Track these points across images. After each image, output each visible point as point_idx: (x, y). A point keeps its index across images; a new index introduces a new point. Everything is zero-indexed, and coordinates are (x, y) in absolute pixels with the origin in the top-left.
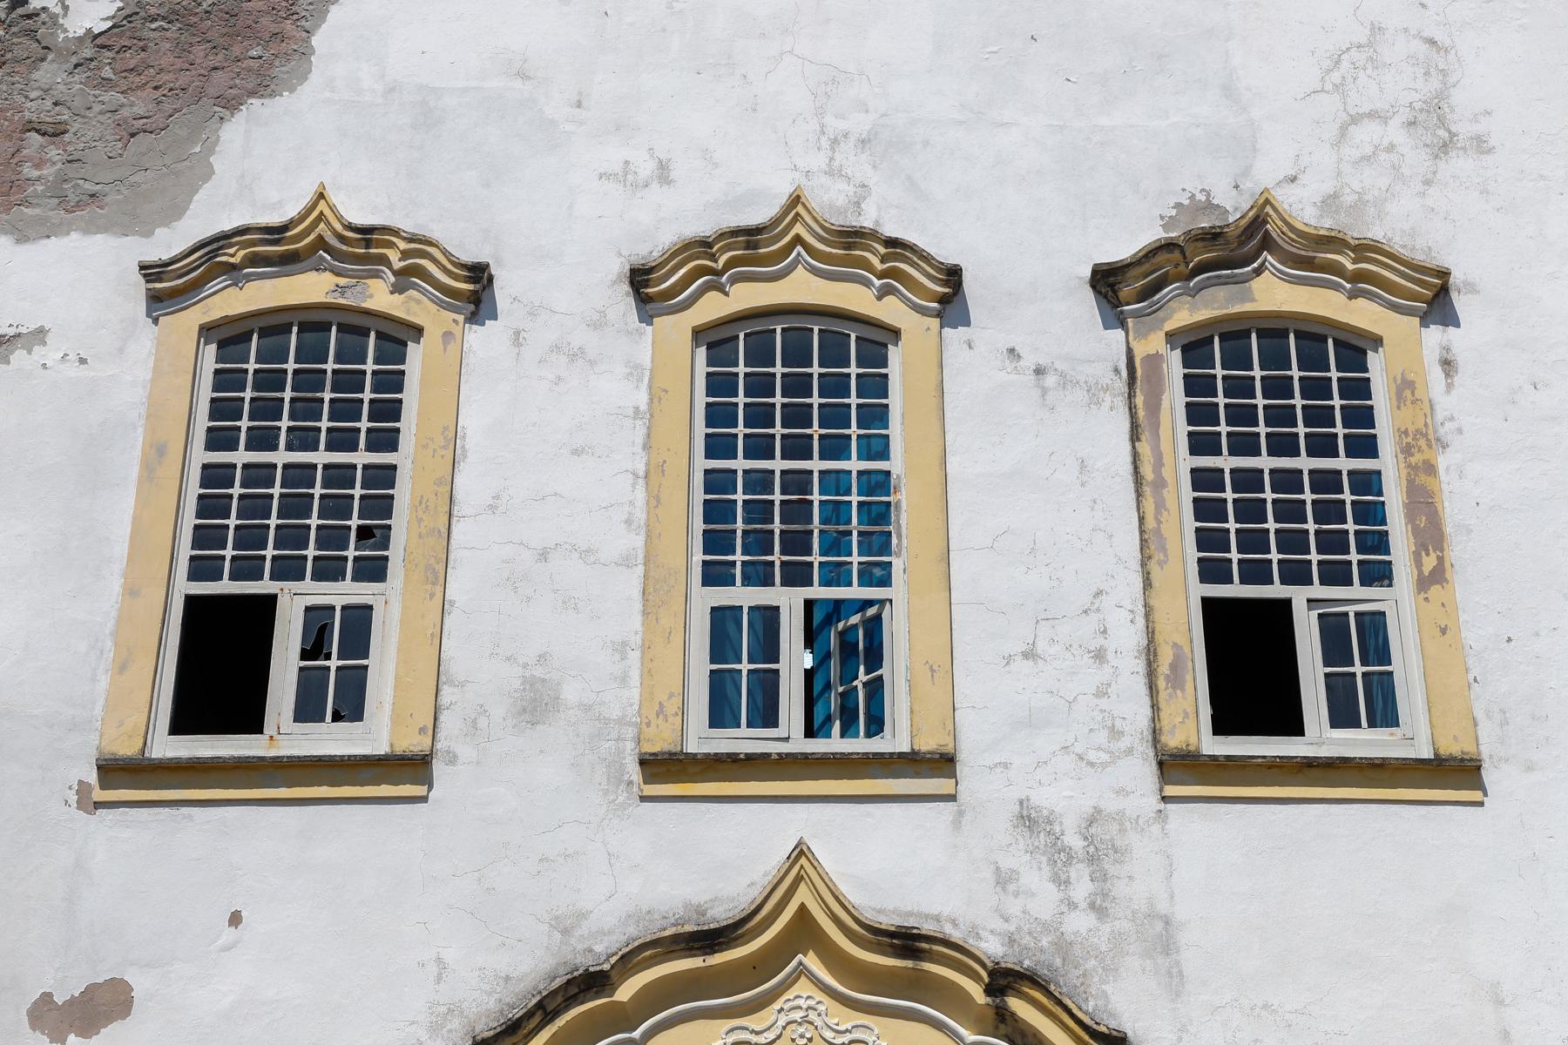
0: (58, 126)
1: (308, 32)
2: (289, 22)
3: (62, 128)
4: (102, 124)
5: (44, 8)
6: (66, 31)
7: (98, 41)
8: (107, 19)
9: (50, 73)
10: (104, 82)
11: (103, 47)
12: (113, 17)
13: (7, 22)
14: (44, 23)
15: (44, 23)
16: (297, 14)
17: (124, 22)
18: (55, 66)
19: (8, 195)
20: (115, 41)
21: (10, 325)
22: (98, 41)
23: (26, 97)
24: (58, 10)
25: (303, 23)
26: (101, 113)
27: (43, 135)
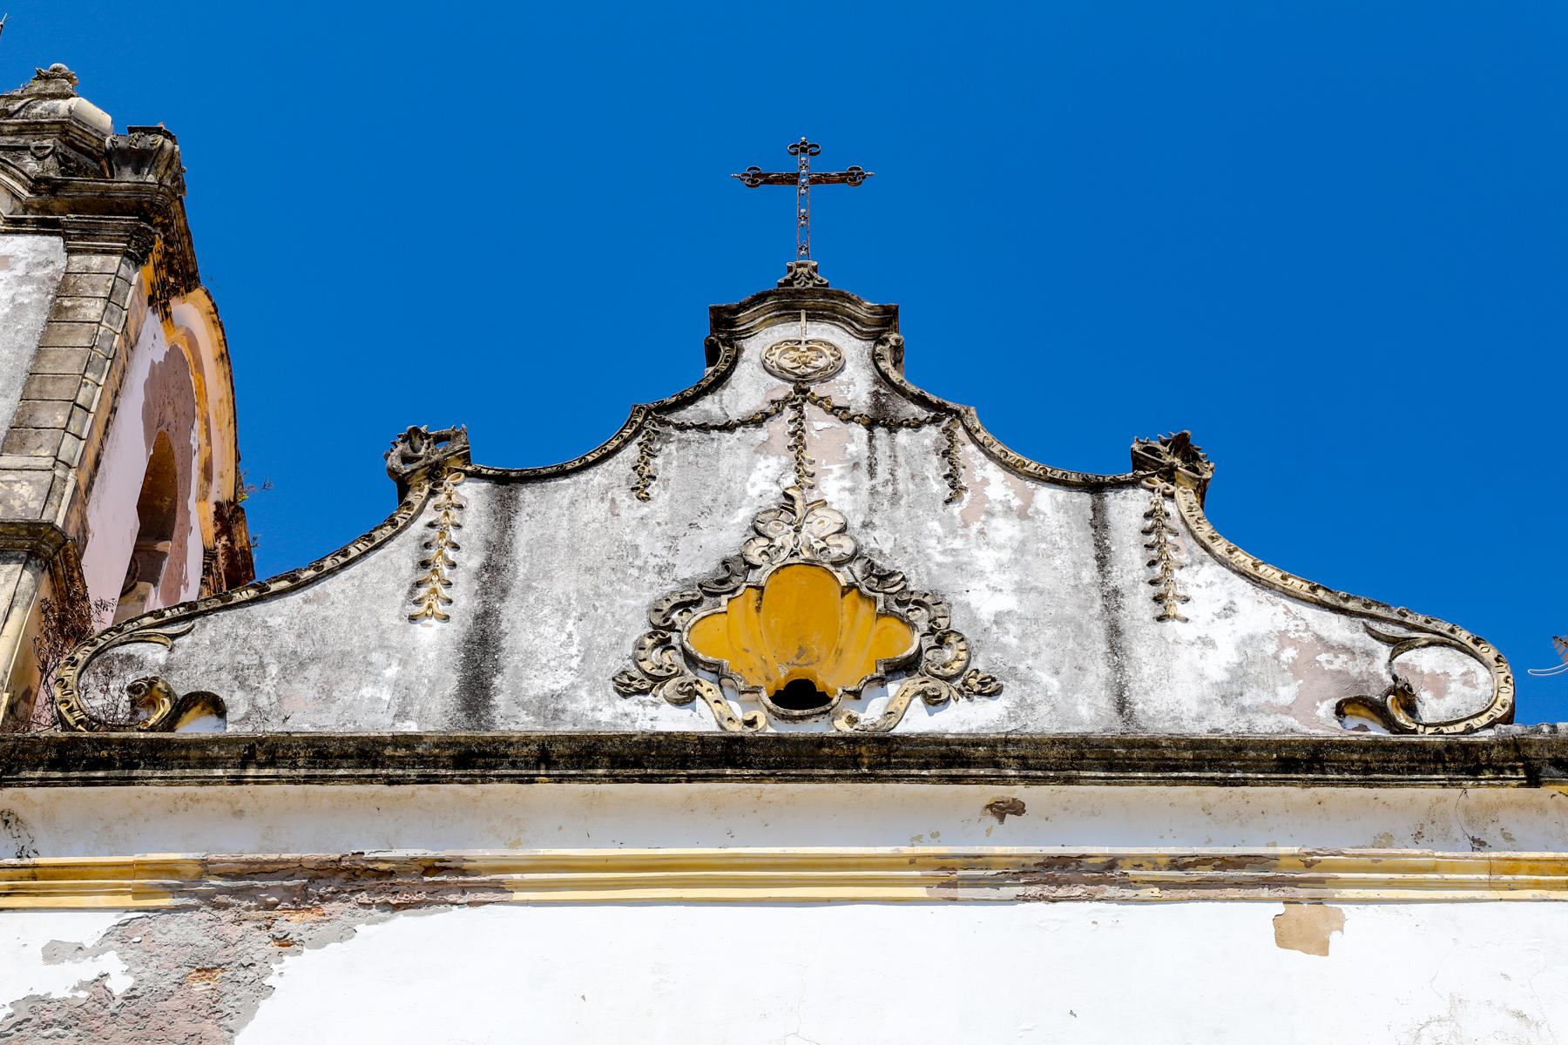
1: (232, 1031)
2: (209, 1021)
16: (221, 1011)
25: (227, 1021)
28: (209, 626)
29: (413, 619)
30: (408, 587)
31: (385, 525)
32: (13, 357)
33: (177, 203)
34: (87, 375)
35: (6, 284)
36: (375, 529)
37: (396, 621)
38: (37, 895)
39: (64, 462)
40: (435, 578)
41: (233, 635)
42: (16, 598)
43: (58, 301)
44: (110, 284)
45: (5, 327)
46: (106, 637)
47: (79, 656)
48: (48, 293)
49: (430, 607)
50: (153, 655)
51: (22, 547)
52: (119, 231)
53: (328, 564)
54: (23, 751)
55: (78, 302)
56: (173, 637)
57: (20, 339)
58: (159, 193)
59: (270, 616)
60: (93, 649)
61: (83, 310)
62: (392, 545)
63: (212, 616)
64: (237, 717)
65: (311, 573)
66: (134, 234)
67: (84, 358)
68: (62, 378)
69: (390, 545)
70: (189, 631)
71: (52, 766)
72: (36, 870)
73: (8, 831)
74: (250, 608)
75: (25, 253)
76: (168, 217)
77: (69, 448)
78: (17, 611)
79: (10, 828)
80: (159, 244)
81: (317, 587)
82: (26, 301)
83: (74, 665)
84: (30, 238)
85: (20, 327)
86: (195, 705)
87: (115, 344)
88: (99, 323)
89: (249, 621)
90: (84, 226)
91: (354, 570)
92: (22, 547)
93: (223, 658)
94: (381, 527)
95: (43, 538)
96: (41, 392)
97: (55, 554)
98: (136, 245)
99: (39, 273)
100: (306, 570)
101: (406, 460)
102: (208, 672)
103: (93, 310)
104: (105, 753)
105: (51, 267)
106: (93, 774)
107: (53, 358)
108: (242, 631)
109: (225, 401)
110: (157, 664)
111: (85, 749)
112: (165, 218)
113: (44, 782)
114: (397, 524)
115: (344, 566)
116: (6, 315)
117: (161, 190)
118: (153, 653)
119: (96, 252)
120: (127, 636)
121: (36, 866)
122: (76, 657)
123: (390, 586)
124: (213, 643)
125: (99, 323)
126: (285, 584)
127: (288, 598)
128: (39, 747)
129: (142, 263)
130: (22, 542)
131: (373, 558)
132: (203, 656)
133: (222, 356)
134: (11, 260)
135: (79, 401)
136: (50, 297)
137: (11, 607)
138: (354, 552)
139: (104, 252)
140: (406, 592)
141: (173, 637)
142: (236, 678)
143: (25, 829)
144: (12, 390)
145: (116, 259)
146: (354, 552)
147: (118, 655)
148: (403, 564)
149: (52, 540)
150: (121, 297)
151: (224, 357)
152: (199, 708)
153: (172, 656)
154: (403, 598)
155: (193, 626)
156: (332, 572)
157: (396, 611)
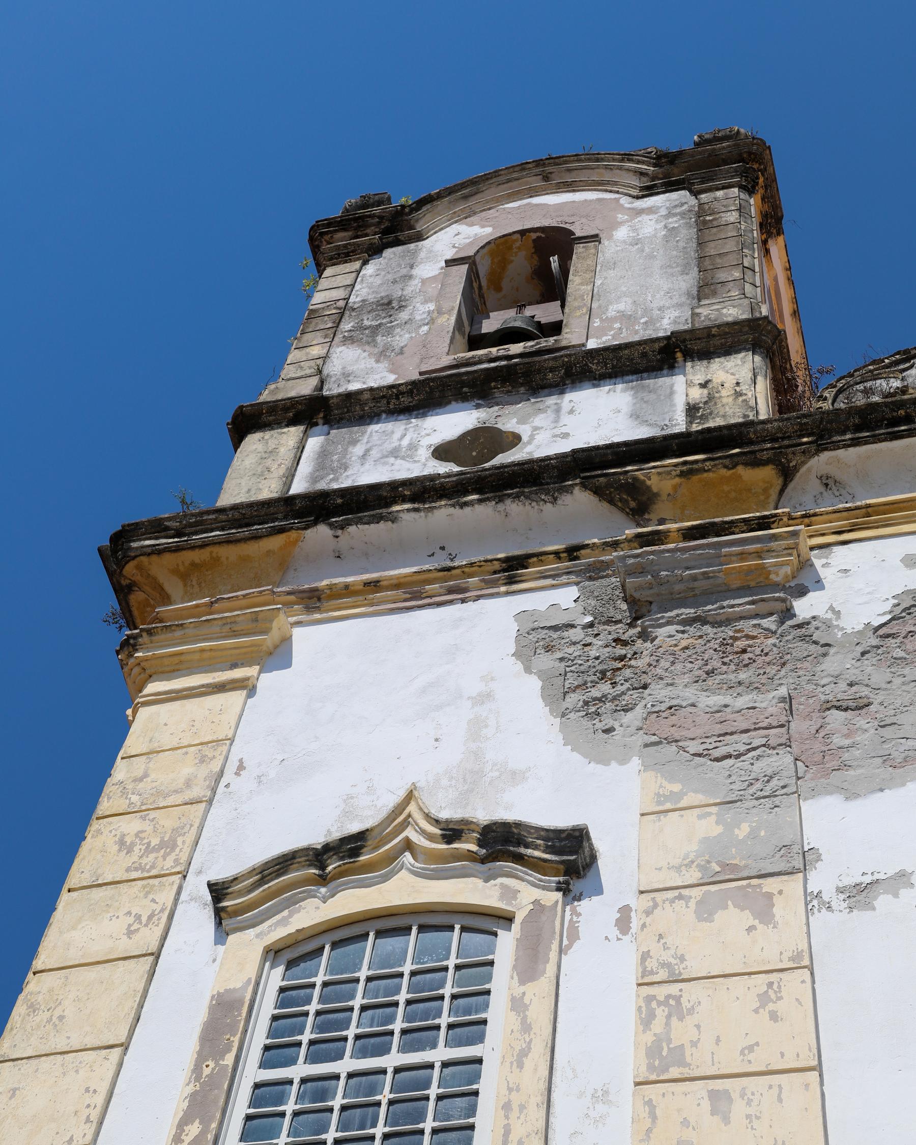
0: (860, 700)
3: (865, 701)
4: (908, 692)
5: (814, 617)
6: (843, 629)
7: (881, 632)
8: (884, 614)
9: (832, 664)
10: (899, 661)
11: (888, 636)
12: (890, 612)
13: (779, 631)
14: (817, 628)
15: (817, 628)
17: (904, 614)
18: (839, 656)
19: (823, 763)
20: (898, 629)
21: (864, 874)
22: (881, 632)
23: (816, 685)
24: (830, 615)
26: (904, 684)
27: (846, 709)
32: (681, 254)
33: (768, 152)
38: (877, 527)
42: (756, 371)
48: (691, 218)
51: (746, 341)
52: (731, 173)
54: (830, 422)
58: (753, 145)
60: (835, 390)
66: (744, 173)
71: (858, 428)
72: (870, 510)
73: (830, 492)
76: (763, 163)
78: (760, 379)
79: (830, 489)
80: (761, 180)
84: (662, 196)
88: (739, 222)
90: (703, 175)
92: (746, 341)
95: (762, 331)
96: (713, 264)
97: (773, 344)
98: (746, 180)
104: (902, 412)
106: (896, 429)
109: (800, 351)
111: (884, 411)
112: (760, 164)
113: (855, 443)
117: (755, 141)
119: (718, 189)
121: (868, 506)
122: (825, 395)
125: (739, 222)
128: (843, 417)
129: (753, 192)
130: (746, 337)
133: (795, 312)
135: (746, 264)
139: (724, 188)
143: (844, 489)
145: (736, 190)
149: (769, 332)
151: (795, 313)
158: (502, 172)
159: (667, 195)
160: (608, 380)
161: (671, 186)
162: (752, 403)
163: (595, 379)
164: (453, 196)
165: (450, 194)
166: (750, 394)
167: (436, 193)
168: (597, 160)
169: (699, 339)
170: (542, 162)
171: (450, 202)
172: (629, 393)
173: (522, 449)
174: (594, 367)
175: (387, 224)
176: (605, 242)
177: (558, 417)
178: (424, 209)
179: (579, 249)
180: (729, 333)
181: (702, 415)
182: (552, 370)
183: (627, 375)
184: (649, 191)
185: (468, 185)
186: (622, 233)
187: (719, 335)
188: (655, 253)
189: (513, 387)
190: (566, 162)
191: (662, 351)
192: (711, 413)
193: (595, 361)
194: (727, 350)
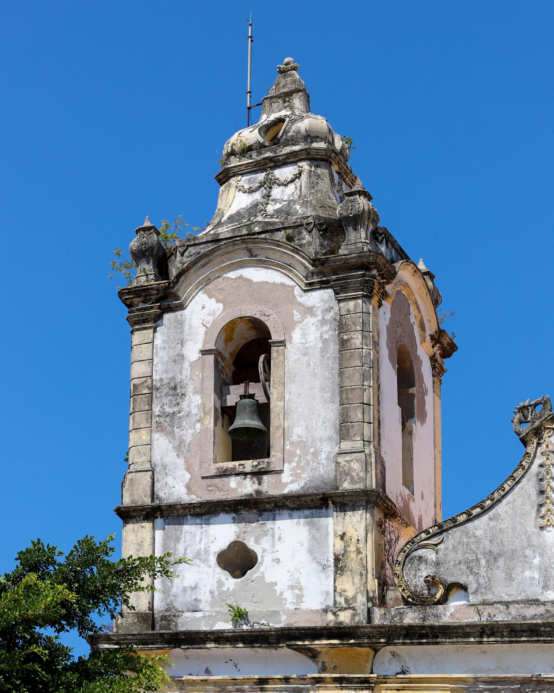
28: (450, 537)
29: (542, 528)
30: (536, 508)
31: (519, 468)
34: (365, 383)
35: (316, 326)
36: (515, 471)
37: (534, 530)
39: (367, 441)
40: (548, 501)
41: (462, 542)
42: (367, 528)
43: (341, 336)
44: (361, 321)
45: (322, 356)
46: (408, 546)
47: (400, 559)
49: (548, 520)
50: (430, 555)
51: (363, 500)
53: (496, 496)
55: (350, 336)
56: (436, 545)
57: (330, 363)
59: (476, 529)
61: (353, 341)
62: (524, 480)
63: (450, 531)
64: (473, 591)
65: (489, 502)
67: (360, 374)
68: (354, 389)
69: (523, 481)
70: (442, 541)
74: (466, 525)
75: (319, 303)
77: (368, 430)
78: (369, 535)
81: (494, 511)
82: (327, 337)
83: (399, 564)
85: (328, 355)
86: (454, 588)
87: (372, 357)
88: (362, 348)
89: (467, 534)
91: (509, 498)
92: (363, 500)
93: (460, 557)
94: (517, 470)
97: (377, 500)
98: (367, 289)
99: (328, 316)
100: (487, 500)
101: (521, 422)
102: (455, 565)
103: (357, 340)
105: (332, 312)
107: (348, 375)
108: (465, 540)
110: (433, 561)
114: (524, 467)
115: (504, 497)
116: (321, 348)
118: (430, 555)
120: (417, 546)
123: (528, 507)
124: (454, 548)
125: (362, 348)
126: (478, 510)
127: (482, 518)
131: (517, 489)
132: (452, 556)
134: (314, 309)
135: (365, 402)
136: (337, 332)
137: (367, 534)
138: (507, 488)
140: (536, 511)
141: (436, 545)
142: (468, 568)
144: (335, 398)
145: (360, 301)
146: (507, 488)
147: (416, 557)
148: (531, 492)
149: (374, 495)
150: (368, 325)
152: (456, 588)
153: (438, 556)
154: (535, 515)
155: (443, 538)
156: (499, 501)
157: (533, 523)
158: (222, 247)
159: (322, 291)
160: (296, 511)
161: (324, 285)
162: (365, 561)
163: (290, 509)
164: (195, 267)
165: (194, 265)
166: (364, 552)
167: (186, 267)
168: (278, 246)
169: (339, 496)
170: (245, 240)
171: (195, 272)
172: (307, 527)
173: (259, 568)
174: (288, 504)
175: (162, 294)
176: (288, 345)
177: (274, 542)
178: (181, 280)
179: (274, 349)
180: (354, 495)
181: (342, 566)
182: (268, 503)
183: (305, 509)
184: (310, 287)
185: (204, 257)
186: (296, 336)
187: (349, 496)
188: (316, 370)
189: (250, 509)
190: (259, 242)
191: (321, 499)
192: (345, 567)
193: (289, 501)
194: (353, 509)
